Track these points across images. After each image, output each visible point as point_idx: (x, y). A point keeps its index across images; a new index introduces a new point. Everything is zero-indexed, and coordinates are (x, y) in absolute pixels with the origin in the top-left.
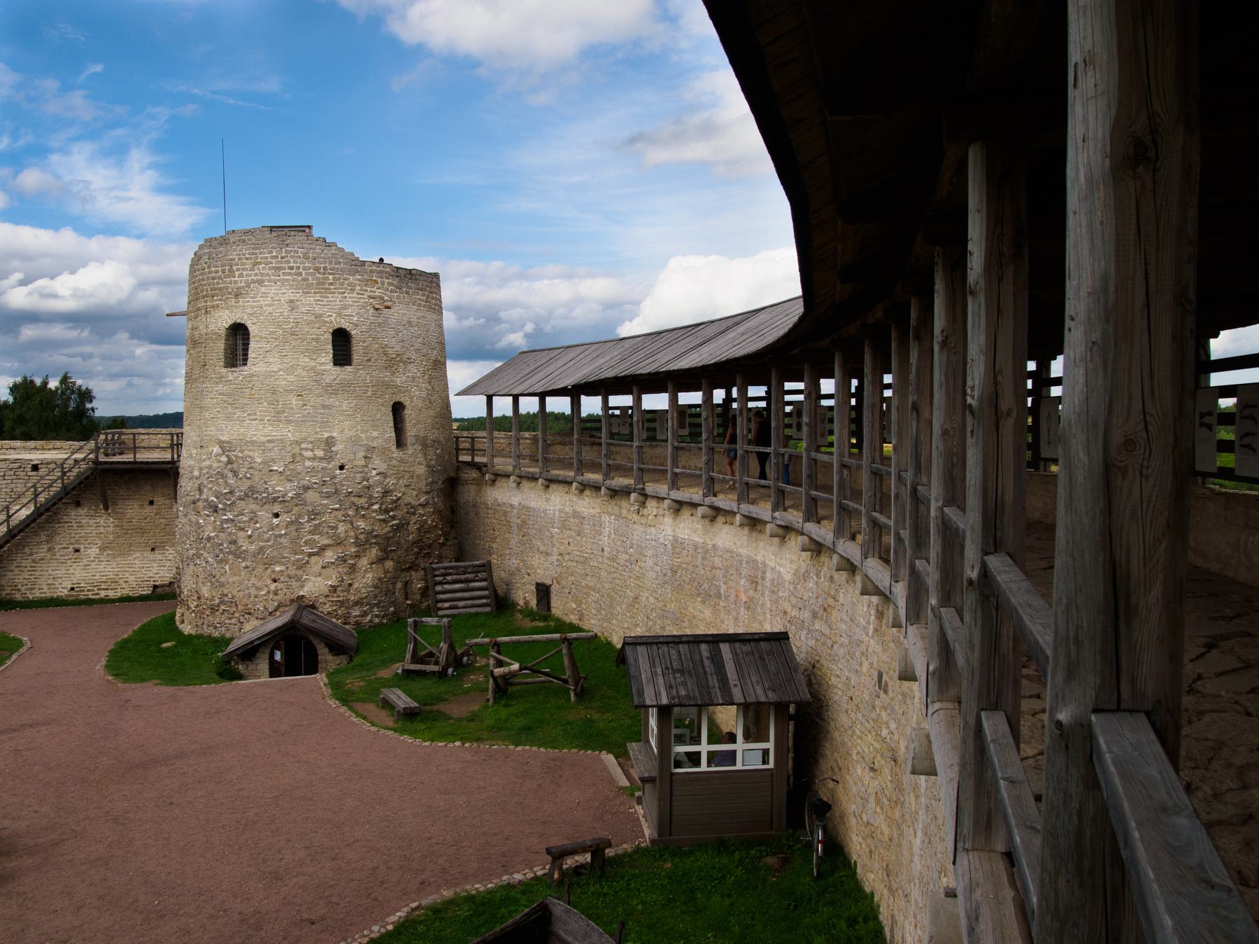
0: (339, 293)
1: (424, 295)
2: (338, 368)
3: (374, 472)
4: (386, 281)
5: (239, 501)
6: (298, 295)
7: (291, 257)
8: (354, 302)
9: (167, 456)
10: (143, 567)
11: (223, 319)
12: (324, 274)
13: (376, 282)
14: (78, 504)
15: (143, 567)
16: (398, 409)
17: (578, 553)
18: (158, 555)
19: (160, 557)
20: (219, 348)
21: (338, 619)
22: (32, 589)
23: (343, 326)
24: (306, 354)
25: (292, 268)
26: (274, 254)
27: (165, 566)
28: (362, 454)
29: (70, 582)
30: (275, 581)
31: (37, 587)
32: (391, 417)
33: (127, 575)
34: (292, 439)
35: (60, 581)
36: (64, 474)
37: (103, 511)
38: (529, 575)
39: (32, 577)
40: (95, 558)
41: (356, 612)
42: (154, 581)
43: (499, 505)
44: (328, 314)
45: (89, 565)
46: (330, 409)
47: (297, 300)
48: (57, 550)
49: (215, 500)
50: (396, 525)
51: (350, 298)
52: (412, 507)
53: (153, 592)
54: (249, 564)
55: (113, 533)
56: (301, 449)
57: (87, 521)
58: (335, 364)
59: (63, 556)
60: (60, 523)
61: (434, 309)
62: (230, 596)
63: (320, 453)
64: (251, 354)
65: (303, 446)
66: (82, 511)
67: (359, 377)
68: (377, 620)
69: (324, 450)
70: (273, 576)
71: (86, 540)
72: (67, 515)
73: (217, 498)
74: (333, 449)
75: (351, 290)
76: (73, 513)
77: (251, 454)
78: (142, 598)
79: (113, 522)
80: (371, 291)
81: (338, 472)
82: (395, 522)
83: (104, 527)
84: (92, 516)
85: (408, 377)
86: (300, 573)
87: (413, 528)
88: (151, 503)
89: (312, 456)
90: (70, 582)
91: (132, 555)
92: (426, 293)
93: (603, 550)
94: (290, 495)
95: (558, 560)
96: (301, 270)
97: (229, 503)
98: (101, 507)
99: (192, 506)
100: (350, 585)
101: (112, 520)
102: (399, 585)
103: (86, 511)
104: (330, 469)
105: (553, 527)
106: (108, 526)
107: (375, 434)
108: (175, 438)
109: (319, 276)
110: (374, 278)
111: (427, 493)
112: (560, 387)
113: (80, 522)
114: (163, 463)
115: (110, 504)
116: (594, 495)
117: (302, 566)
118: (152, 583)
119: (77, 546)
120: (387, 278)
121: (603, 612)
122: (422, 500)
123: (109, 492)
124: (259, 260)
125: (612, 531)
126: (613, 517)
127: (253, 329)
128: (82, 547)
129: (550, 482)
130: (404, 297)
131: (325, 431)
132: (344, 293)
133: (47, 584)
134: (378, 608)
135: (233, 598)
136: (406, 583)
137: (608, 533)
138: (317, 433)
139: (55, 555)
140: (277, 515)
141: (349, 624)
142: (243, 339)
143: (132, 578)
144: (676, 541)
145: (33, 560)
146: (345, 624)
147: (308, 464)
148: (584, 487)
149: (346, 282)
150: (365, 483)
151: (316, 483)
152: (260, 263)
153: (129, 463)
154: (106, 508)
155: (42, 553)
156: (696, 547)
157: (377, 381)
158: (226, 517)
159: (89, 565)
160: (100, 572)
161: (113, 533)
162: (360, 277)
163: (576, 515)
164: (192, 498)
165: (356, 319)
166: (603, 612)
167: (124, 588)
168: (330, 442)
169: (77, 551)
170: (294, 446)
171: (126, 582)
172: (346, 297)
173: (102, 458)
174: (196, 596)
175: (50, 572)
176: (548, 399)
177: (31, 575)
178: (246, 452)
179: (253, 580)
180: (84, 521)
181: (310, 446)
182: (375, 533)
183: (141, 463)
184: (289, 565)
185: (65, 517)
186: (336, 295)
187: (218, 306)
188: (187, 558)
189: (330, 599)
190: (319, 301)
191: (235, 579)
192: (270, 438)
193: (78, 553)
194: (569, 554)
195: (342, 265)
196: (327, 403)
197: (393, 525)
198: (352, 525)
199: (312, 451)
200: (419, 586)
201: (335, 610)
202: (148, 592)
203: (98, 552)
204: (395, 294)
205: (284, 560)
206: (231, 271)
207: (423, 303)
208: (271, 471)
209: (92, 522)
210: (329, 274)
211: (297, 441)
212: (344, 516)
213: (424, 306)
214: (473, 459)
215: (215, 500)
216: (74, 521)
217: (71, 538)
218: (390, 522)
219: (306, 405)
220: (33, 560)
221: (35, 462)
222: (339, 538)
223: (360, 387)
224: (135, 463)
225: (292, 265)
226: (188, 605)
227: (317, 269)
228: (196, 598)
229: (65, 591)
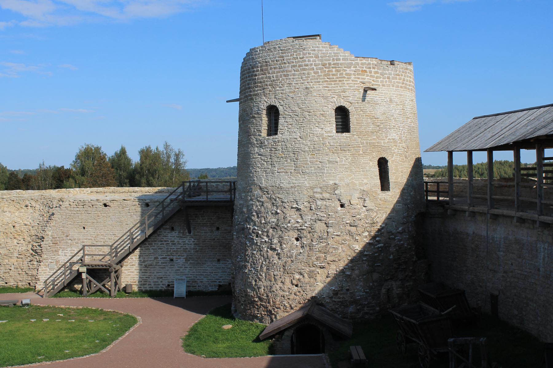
0: (340, 81)
1: (400, 79)
2: (340, 134)
3: (364, 208)
4: (373, 70)
5: (271, 229)
6: (311, 84)
7: (307, 57)
8: (351, 87)
9: (227, 196)
10: (212, 273)
12: (329, 68)
13: (365, 71)
14: (173, 229)
15: (212, 273)
16: (383, 164)
17: (519, 272)
19: (223, 266)
21: (339, 314)
22: (144, 284)
23: (342, 104)
24: (317, 125)
25: (307, 65)
26: (295, 56)
27: (226, 272)
28: (357, 195)
29: (167, 281)
30: (297, 286)
31: (147, 283)
32: (376, 170)
33: (202, 277)
34: (307, 185)
35: (161, 280)
36: (164, 208)
37: (187, 234)
38: (481, 287)
39: (145, 277)
40: (183, 265)
41: (351, 309)
42: (219, 282)
44: (333, 96)
45: (179, 270)
46: (333, 164)
47: (311, 88)
48: (159, 259)
49: (256, 228)
50: (381, 247)
51: (348, 84)
52: (393, 234)
53: (218, 289)
54: (278, 273)
55: (194, 249)
56: (314, 192)
57: (178, 240)
58: (337, 132)
59: (164, 263)
60: (162, 241)
61: (408, 89)
62: (265, 295)
63: (326, 195)
64: (280, 127)
65: (315, 190)
66: (175, 234)
67: (354, 140)
68: (367, 317)
69: (329, 193)
70: (295, 282)
71: (177, 253)
72: (166, 236)
73: (258, 227)
74: (336, 192)
75: (348, 78)
76: (169, 235)
77: (279, 196)
78: (211, 293)
79: (194, 242)
80: (362, 79)
81: (340, 208)
82: (380, 245)
83: (188, 244)
84: (181, 237)
85: (389, 139)
86: (312, 280)
87: (392, 249)
88: (218, 229)
89: (322, 198)
90: (167, 281)
91: (205, 264)
92: (403, 77)
93: (539, 270)
94: (306, 225)
95: (503, 276)
96: (313, 66)
97: (265, 230)
98: (187, 231)
99: (242, 231)
100: (348, 290)
101: (193, 240)
102: (384, 291)
103: (177, 234)
104: (334, 207)
105: (499, 251)
106: (191, 244)
107: (365, 181)
108: (232, 184)
109: (325, 69)
110: (364, 69)
111: (404, 224)
112: (502, 144)
113: (174, 241)
114: (225, 201)
115: (192, 229)
116: (532, 227)
118: (218, 283)
119: (171, 257)
120: (374, 68)
121: (539, 319)
122: (400, 229)
123: (191, 221)
124: (285, 61)
125: (546, 255)
126: (547, 245)
127: (281, 109)
128: (175, 257)
129: (495, 217)
130: (386, 82)
131: (330, 180)
132: (343, 81)
133: (153, 282)
134: (368, 307)
135: (267, 296)
136: (388, 290)
137: (542, 257)
138: (324, 181)
139: (159, 263)
140: (297, 239)
141: (347, 318)
142: (275, 116)
143: (205, 280)
145: (145, 265)
146: (344, 318)
147: (319, 203)
148: (522, 221)
149: (344, 73)
150: (358, 216)
151: (324, 217)
152: (285, 63)
153: (204, 201)
154: (190, 232)
155: (150, 261)
157: (367, 143)
158: (264, 240)
159: (179, 270)
160: (186, 275)
161: (194, 249)
162: (354, 69)
164: (242, 226)
165: (351, 99)
166: (539, 319)
167: (200, 286)
168: (335, 187)
169: (172, 260)
170: (308, 190)
171: (201, 282)
172: (344, 84)
173: (186, 199)
174: (244, 294)
175: (155, 274)
176: (495, 153)
177: (144, 275)
178: (277, 195)
179: (280, 285)
180: (176, 241)
181: (319, 190)
182: (366, 253)
183: (211, 201)
184: (306, 275)
185: (164, 238)
186: (338, 82)
188: (239, 267)
189: (334, 299)
190: (327, 87)
191: (269, 283)
192: (292, 185)
193: (172, 262)
194: (512, 272)
195: (341, 62)
196: (330, 160)
197: (379, 247)
198: (350, 247)
199: (321, 194)
200: (397, 292)
201: (337, 309)
202: (216, 289)
203: (184, 261)
204: (379, 80)
205: (302, 271)
206: (267, 70)
207: (400, 85)
208: (292, 208)
209: (181, 241)
210: (332, 67)
211: (311, 187)
212: (344, 240)
213: (401, 87)
214: (438, 198)
215: (256, 228)
216: (170, 240)
217: (168, 251)
218: (376, 245)
219: (317, 161)
220: (145, 265)
221: (147, 201)
222: (339, 256)
223: (354, 147)
224: (207, 201)
225: (307, 63)
226: (239, 299)
227: (324, 65)
228: (244, 295)
229: (164, 286)
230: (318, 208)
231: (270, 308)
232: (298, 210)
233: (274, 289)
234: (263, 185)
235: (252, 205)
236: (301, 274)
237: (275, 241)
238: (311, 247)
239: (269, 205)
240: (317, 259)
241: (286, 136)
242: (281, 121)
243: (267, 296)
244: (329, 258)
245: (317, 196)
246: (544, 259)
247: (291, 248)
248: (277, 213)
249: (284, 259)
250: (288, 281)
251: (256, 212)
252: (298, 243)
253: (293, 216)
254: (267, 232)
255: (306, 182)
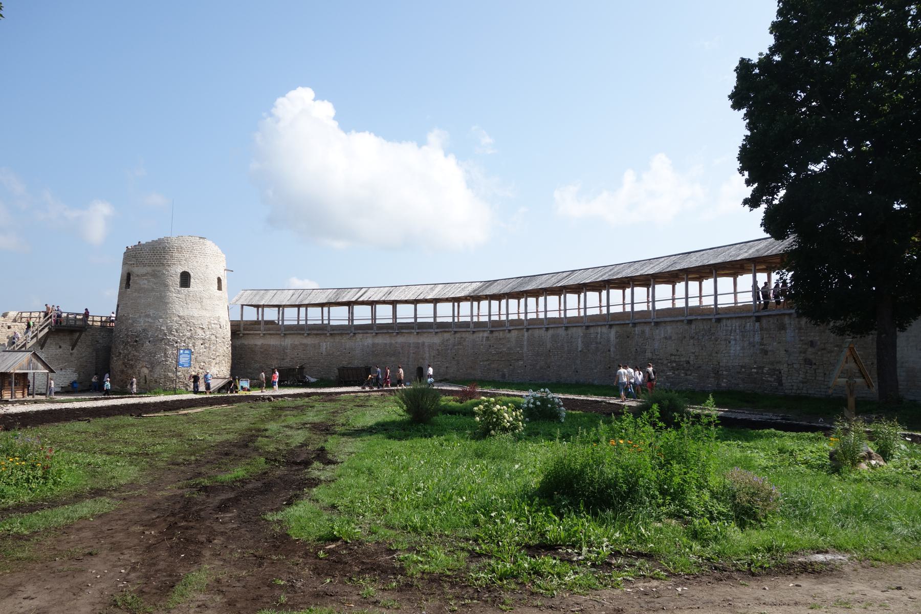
11: (180, 270)
18: (63, 372)
20: (178, 280)
30: (202, 369)
43: (245, 345)
63: (216, 322)
64: (191, 284)
88: (60, 347)
116: (315, 337)
117: (210, 363)
126: (328, 343)
127: (192, 274)
135: (184, 376)
140: (202, 344)
144: (374, 345)
147: (213, 325)
154: (41, 349)
156: (386, 344)
163: (301, 344)
179: (193, 369)
187: (174, 264)
230: (212, 329)
231: (186, 382)
232: (203, 329)
233: (190, 371)
234: (181, 314)
235: (172, 326)
236: (204, 362)
237: (191, 345)
238: (209, 348)
239: (184, 325)
240: (212, 354)
241: (196, 289)
242: (192, 280)
243: (184, 376)
244: (217, 354)
245: (212, 322)
246: (326, 348)
247: (200, 349)
248: (191, 330)
249: (195, 355)
250: (197, 366)
251: (176, 329)
252: (202, 346)
253: (200, 332)
254: (185, 340)
255: (207, 314)
